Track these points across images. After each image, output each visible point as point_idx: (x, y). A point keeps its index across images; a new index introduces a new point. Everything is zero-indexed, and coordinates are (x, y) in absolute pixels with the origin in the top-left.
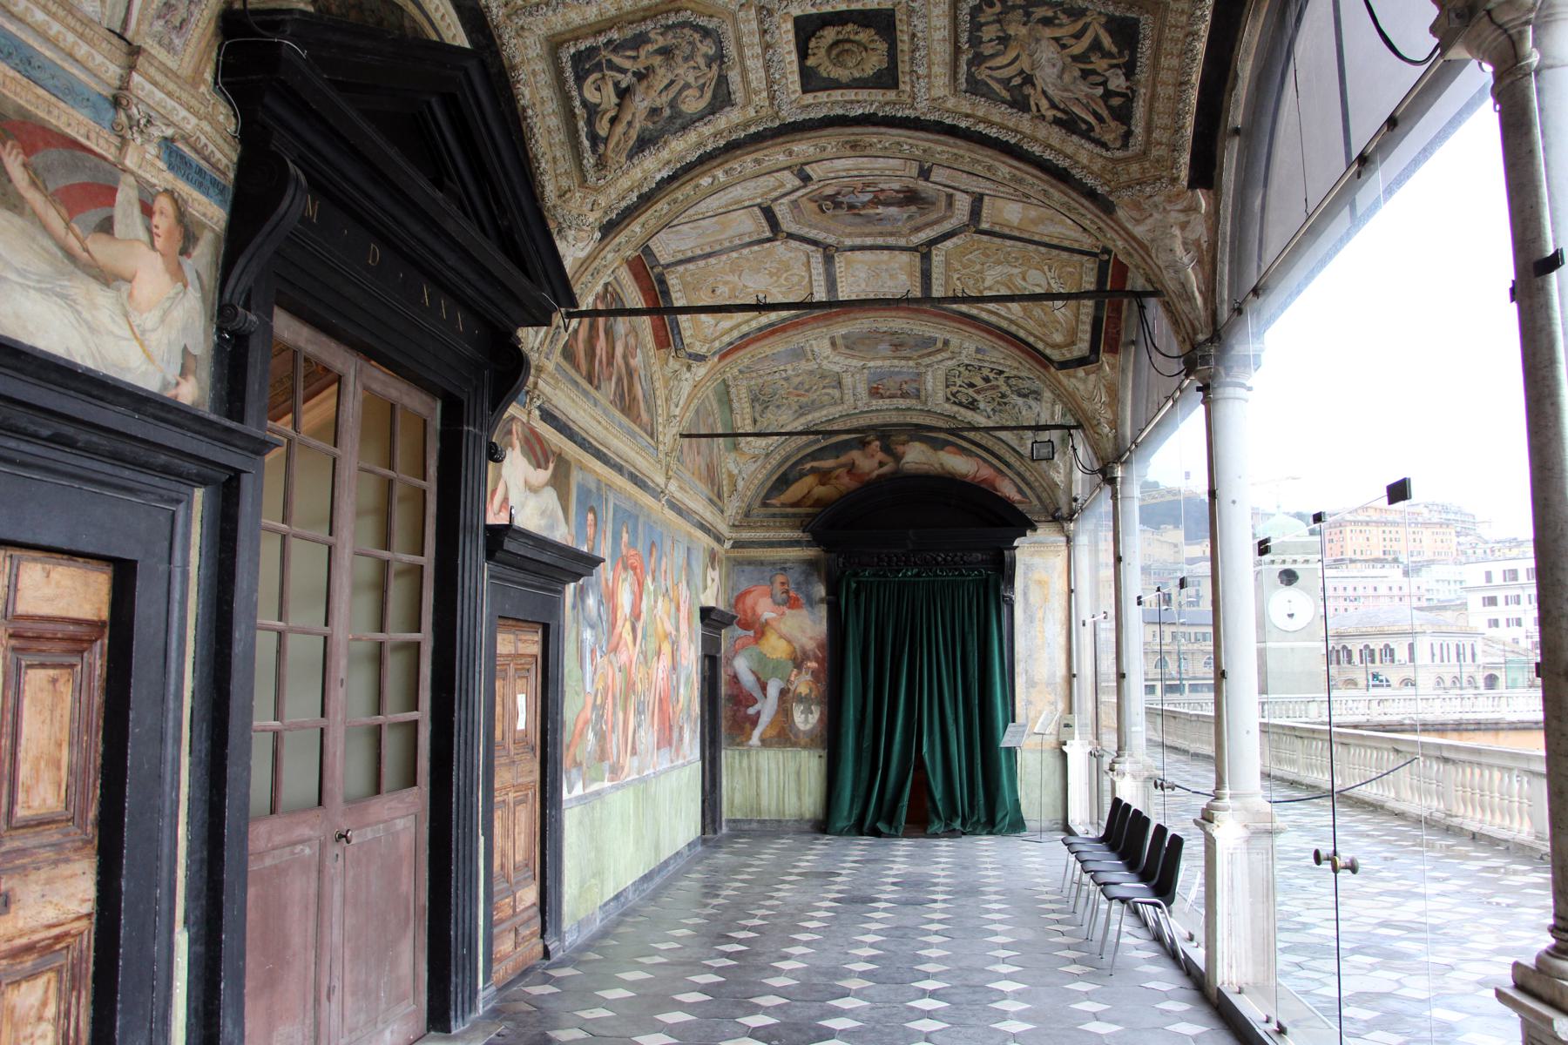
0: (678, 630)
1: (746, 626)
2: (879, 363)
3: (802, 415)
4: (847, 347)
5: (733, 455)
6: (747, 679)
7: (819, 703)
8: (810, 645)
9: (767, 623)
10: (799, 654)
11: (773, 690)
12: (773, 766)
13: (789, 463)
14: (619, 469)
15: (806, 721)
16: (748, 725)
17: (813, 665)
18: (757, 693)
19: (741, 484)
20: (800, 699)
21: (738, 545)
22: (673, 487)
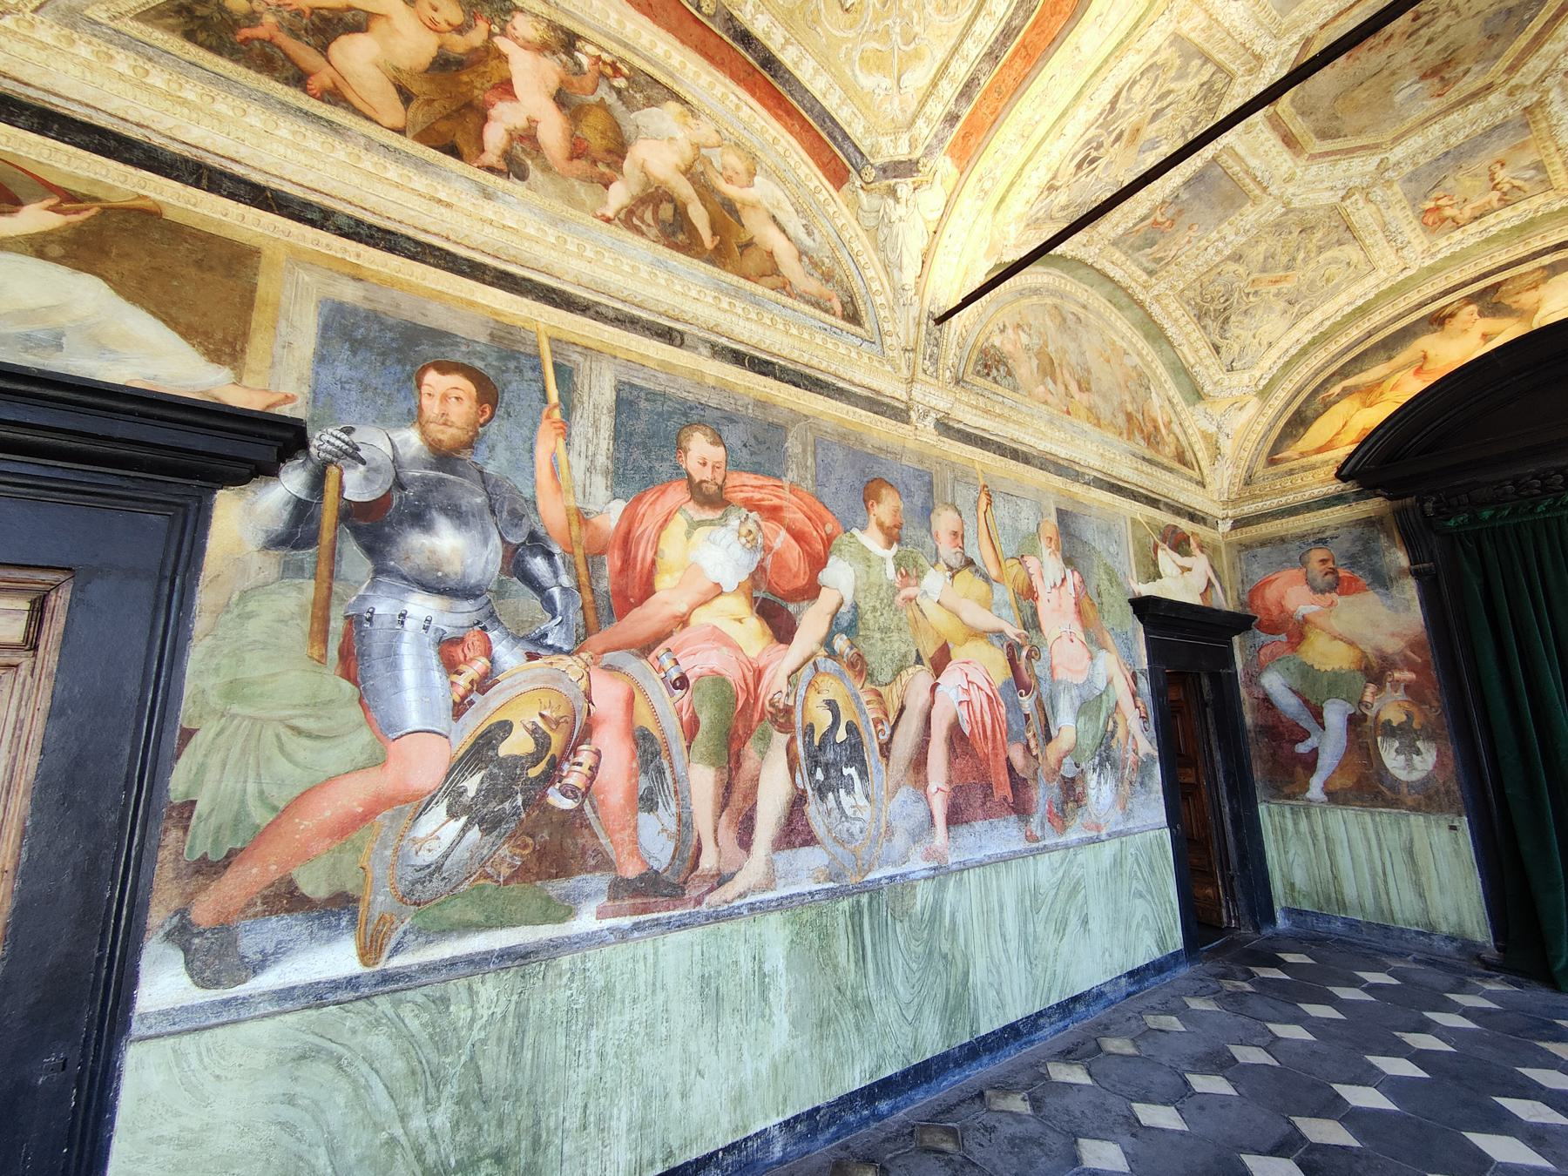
0: (1032, 623)
1: (1273, 628)
2: (1415, 142)
3: (1300, 316)
4: (1323, 135)
5: (1200, 407)
6: (1287, 702)
7: (1430, 738)
8: (1393, 646)
9: (1305, 620)
10: (1372, 659)
11: (1335, 714)
12: (1356, 833)
13: (1304, 395)
14: (667, 335)
15: (1410, 765)
16: (1299, 769)
17: (1409, 676)
18: (1306, 722)
19: (1227, 446)
20: (1390, 730)
21: (1239, 523)
22: (282, 150)
